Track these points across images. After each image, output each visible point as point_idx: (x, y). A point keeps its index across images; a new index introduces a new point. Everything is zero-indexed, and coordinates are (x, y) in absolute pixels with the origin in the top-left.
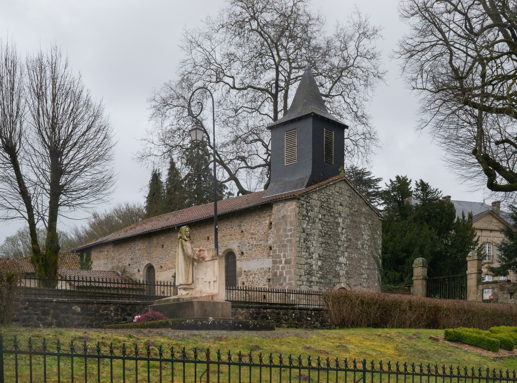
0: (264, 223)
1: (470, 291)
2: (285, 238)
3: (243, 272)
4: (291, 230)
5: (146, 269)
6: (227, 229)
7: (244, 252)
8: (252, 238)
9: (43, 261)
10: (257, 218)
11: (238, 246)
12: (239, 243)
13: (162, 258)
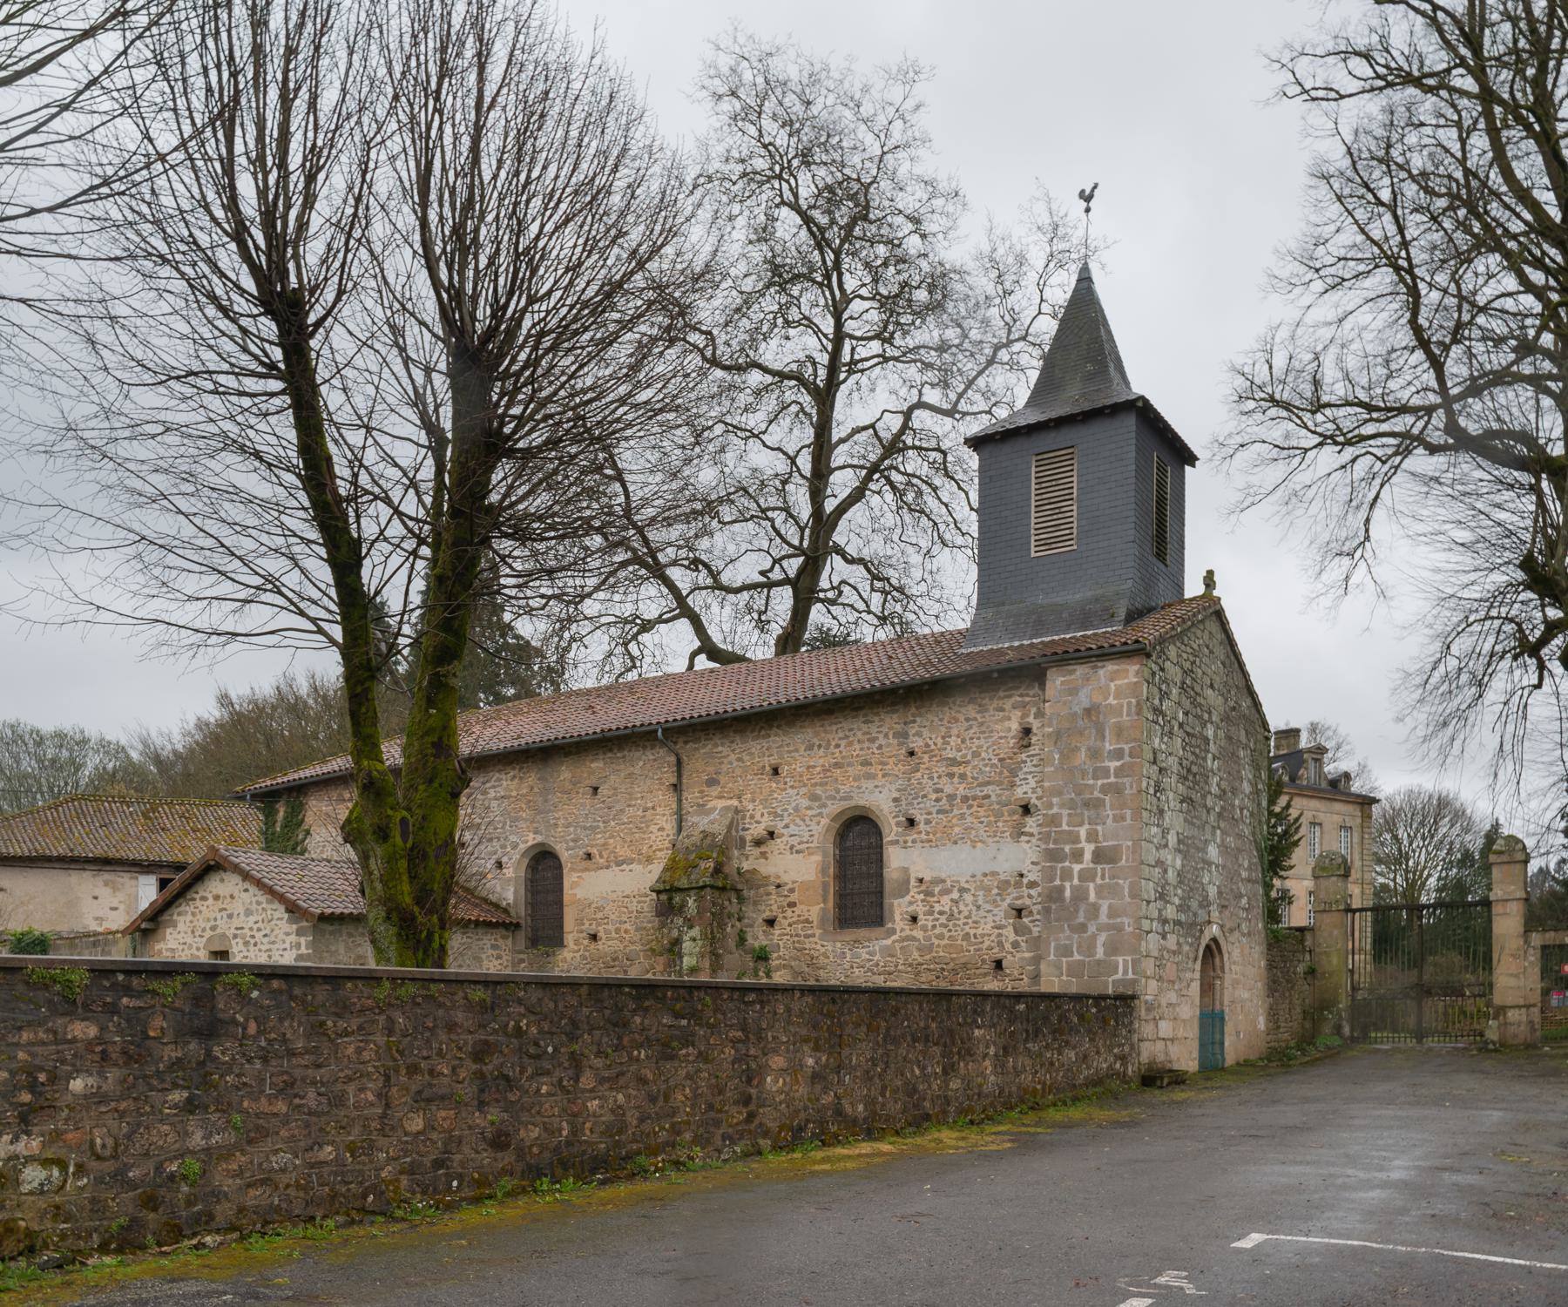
0: (998, 727)
1: (1502, 948)
2: (1095, 778)
3: (913, 882)
4: (1118, 754)
5: (526, 861)
6: (850, 744)
7: (920, 818)
8: (951, 776)
9: (404, 837)
10: (971, 711)
11: (896, 800)
12: (899, 790)
13: (593, 829)
